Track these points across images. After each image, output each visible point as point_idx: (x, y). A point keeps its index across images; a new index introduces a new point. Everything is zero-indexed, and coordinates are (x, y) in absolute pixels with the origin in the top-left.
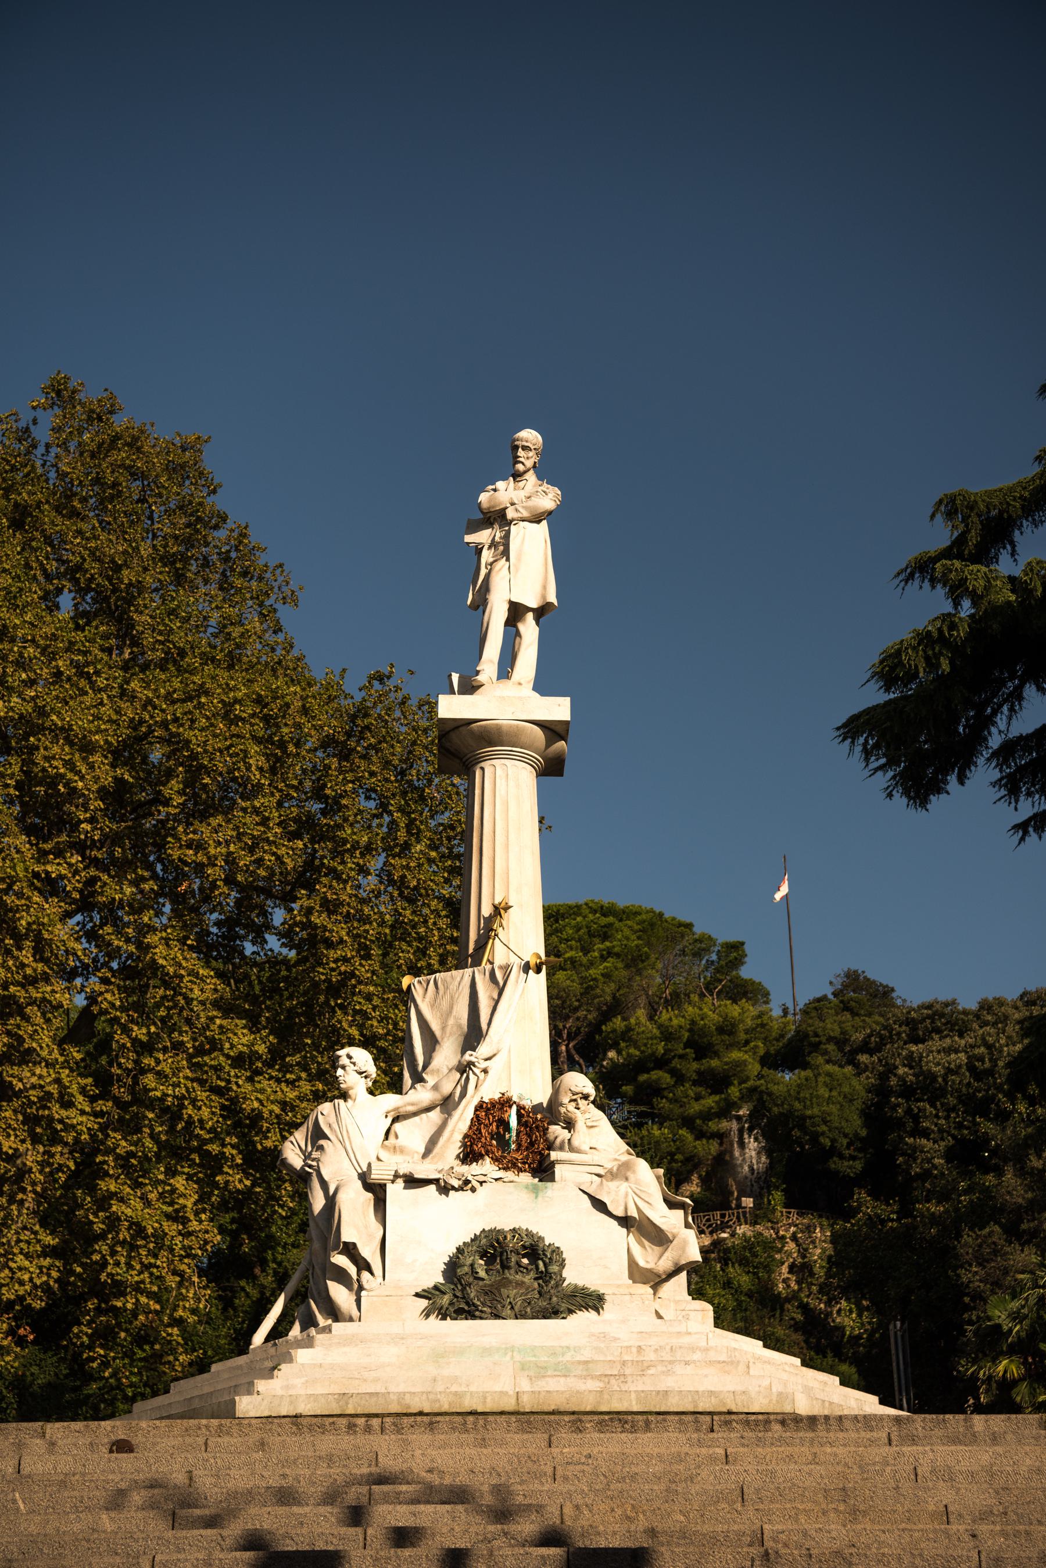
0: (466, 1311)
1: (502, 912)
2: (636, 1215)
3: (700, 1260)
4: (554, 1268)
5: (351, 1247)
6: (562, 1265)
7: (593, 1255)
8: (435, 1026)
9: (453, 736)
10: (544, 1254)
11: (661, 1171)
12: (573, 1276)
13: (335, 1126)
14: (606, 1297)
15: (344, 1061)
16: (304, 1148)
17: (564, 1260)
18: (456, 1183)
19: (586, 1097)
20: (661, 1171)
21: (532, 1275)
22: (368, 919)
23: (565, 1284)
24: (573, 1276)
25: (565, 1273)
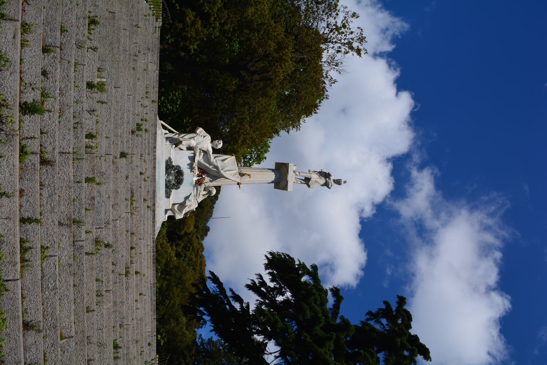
0: (167, 169)
6: (176, 189)
7: (177, 196)
8: (225, 161)
19: (210, 194)
24: (173, 191)
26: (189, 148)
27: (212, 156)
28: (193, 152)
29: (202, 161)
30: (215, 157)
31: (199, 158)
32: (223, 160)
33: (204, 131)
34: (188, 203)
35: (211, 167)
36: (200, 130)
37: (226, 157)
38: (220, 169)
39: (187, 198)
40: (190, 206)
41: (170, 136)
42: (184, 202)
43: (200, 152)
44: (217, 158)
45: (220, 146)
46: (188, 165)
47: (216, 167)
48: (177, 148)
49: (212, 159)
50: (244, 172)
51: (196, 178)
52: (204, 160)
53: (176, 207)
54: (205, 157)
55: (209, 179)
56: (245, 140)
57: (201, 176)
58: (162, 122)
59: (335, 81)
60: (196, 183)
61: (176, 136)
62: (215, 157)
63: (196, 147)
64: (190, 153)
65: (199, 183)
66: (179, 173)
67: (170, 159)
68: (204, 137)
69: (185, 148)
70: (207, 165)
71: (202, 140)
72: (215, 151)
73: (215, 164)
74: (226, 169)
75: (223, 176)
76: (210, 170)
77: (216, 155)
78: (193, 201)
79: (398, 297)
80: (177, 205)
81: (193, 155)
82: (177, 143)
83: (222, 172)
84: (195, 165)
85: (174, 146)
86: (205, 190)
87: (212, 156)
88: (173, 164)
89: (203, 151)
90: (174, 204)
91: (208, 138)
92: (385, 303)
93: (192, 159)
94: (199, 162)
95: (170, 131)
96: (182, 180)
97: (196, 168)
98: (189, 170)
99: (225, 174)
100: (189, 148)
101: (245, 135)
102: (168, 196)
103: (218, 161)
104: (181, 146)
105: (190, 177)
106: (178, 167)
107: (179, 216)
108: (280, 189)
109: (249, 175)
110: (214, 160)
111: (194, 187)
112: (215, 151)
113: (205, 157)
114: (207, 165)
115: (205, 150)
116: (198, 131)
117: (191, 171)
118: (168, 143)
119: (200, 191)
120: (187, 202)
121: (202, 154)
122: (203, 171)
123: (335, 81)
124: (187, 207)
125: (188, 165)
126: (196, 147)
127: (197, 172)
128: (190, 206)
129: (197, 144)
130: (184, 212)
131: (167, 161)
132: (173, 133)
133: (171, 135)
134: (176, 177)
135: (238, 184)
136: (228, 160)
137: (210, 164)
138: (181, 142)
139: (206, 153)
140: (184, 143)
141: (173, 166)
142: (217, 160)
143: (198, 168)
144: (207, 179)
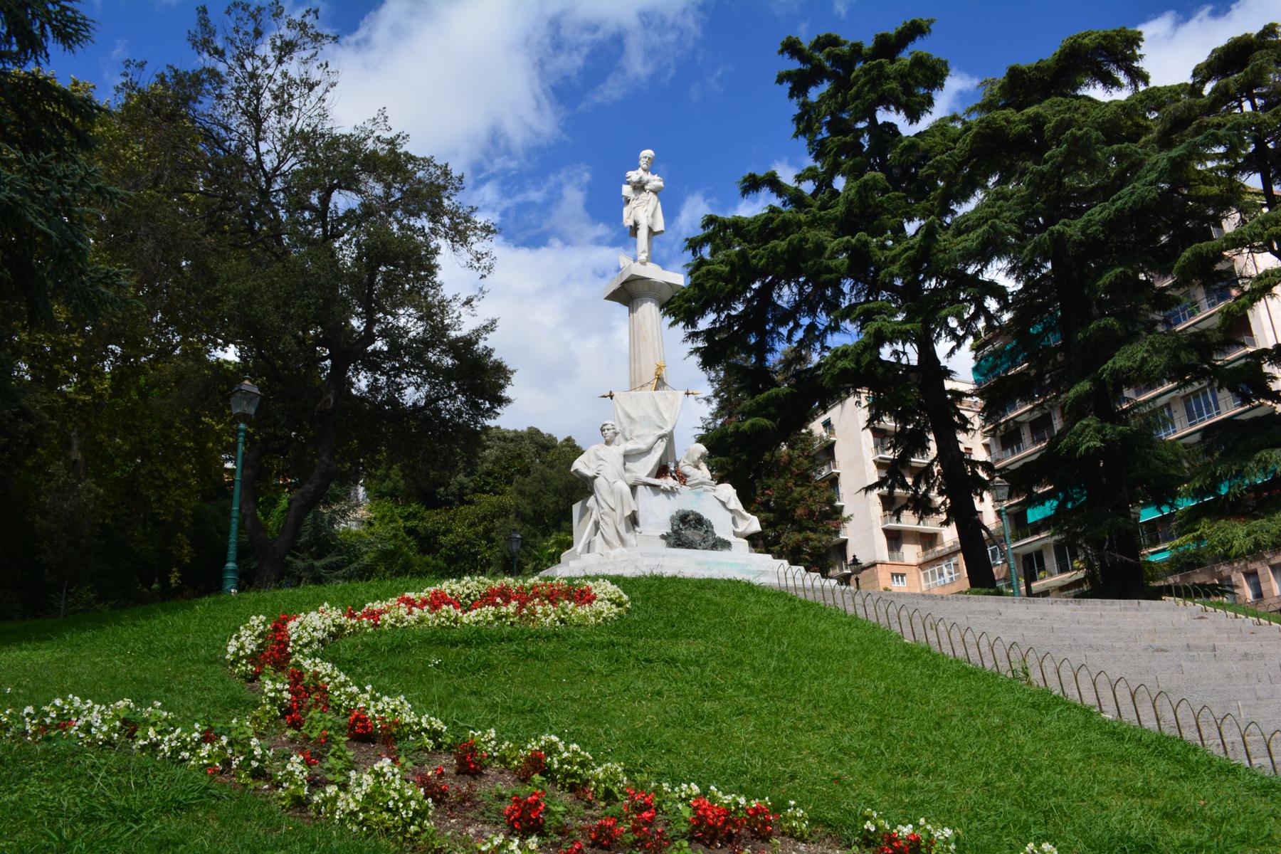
8: (633, 415)
9: (632, 285)
28: (640, 488)
33: (581, 458)
38: (662, 432)
59: (382, 111)
67: (663, 537)
73: (651, 440)
79: (781, 52)
90: (736, 534)
92: (781, 79)
102: (726, 545)
109: (660, 368)
115: (621, 460)
116: (590, 473)
123: (382, 111)
129: (622, 478)
130: (745, 513)
131: (670, 545)
136: (628, 409)
137: (648, 451)
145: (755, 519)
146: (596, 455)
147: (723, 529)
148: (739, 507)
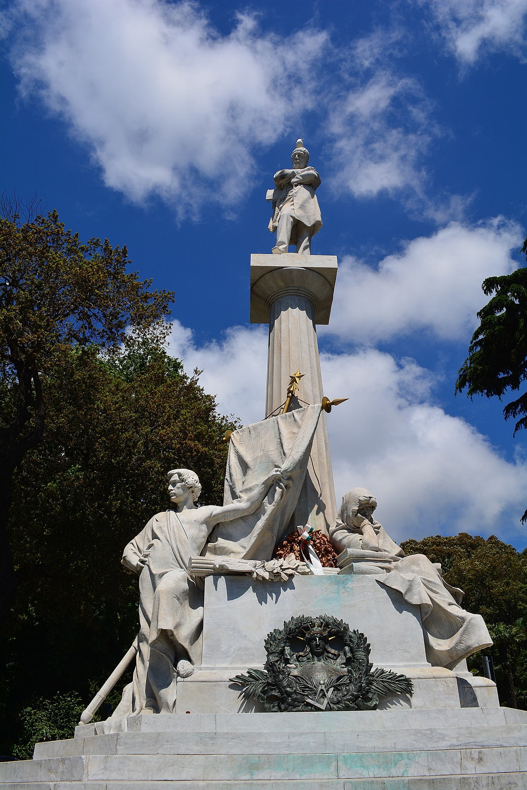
1: (297, 379)
2: (430, 603)
3: (492, 643)
4: (360, 654)
5: (169, 634)
6: (368, 651)
8: (248, 459)
10: (351, 641)
11: (439, 565)
12: (379, 661)
13: (165, 529)
14: (413, 682)
15: (175, 478)
16: (141, 547)
17: (369, 645)
18: (267, 576)
20: (439, 565)
21: (342, 659)
22: (207, 408)
23: (373, 670)
25: (372, 659)
26: (195, 595)
27: (230, 505)
28: (209, 581)
29: (248, 542)
30: (235, 496)
31: (235, 555)
32: (245, 467)
33: (137, 539)
34: (420, 596)
35: (269, 508)
36: (131, 554)
37: (232, 460)
39: (399, 599)
40: (427, 584)
41: (144, 681)
42: (418, 610)
43: (216, 551)
44: (238, 489)
45: (191, 476)
46: (262, 599)
47: (269, 488)
48: (193, 652)
49: (242, 504)
50: (284, 398)
51: (316, 566)
52: (246, 534)
53: (441, 645)
54: (231, 530)
55: (312, 515)
56: (199, 437)
57: (304, 544)
58: (88, 712)
60: (334, 564)
61: (146, 649)
62: (235, 496)
63: (189, 567)
64: (215, 592)
65: (332, 552)
66: (300, 638)
68: (155, 536)
69: (194, 616)
70: (260, 524)
71: (166, 545)
72: (211, 494)
73: (256, 492)
74: (274, 454)
75: (303, 462)
76: (280, 510)
77: (227, 495)
78: (409, 576)
80: (433, 641)
81: (222, 581)
82: (171, 652)
83: (286, 465)
84: (263, 569)
85: (183, 665)
86: (357, 530)
87: (230, 504)
88: (260, 665)
89: (211, 538)
91: (160, 521)
93: (237, 582)
94: (252, 555)
95: (127, 677)
96: (326, 623)
97: (274, 564)
98: (286, 594)
99: (295, 454)
100: (195, 595)
101: (186, 434)
103: (248, 485)
104: (183, 636)
105: (314, 592)
106: (271, 641)
107: (479, 632)
108: (330, 299)
109: (293, 380)
110: (244, 496)
111: (351, 570)
112: (211, 494)
113: (231, 530)
114: (260, 524)
117: (288, 584)
118: (169, 694)
119: (365, 546)
120: (415, 600)
121: (221, 542)
122: (285, 538)
124: (438, 600)
125: (262, 599)
126: (189, 567)
127: (291, 561)
128: (427, 584)
130: (457, 611)
132: (132, 664)
133: (141, 670)
134: (318, 653)
135: (327, 407)
138: (166, 636)
139: (216, 530)
140: (166, 623)
141: (269, 666)
142: (244, 487)
143: (275, 556)
144: (315, 522)
145: (478, 619)
146: (153, 531)
147: (395, 646)
148: (445, 599)
